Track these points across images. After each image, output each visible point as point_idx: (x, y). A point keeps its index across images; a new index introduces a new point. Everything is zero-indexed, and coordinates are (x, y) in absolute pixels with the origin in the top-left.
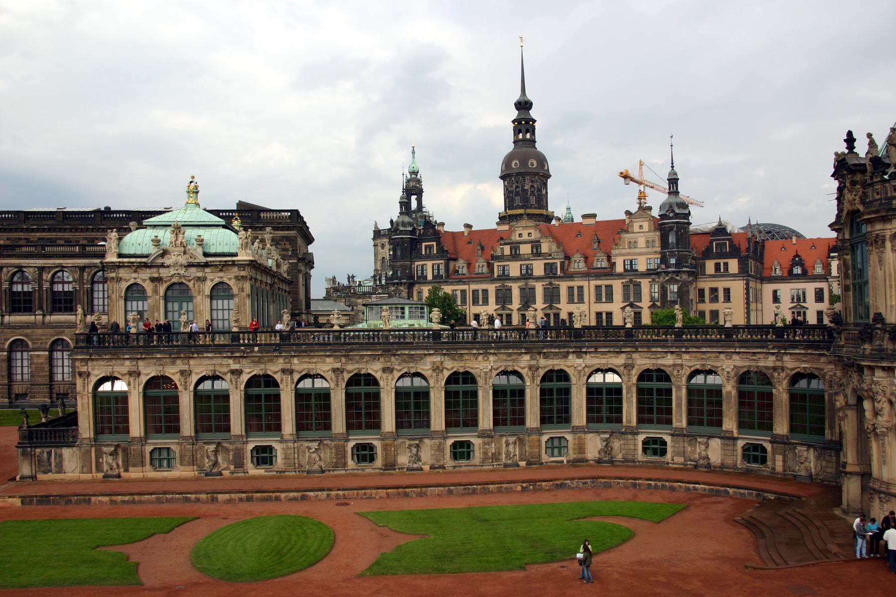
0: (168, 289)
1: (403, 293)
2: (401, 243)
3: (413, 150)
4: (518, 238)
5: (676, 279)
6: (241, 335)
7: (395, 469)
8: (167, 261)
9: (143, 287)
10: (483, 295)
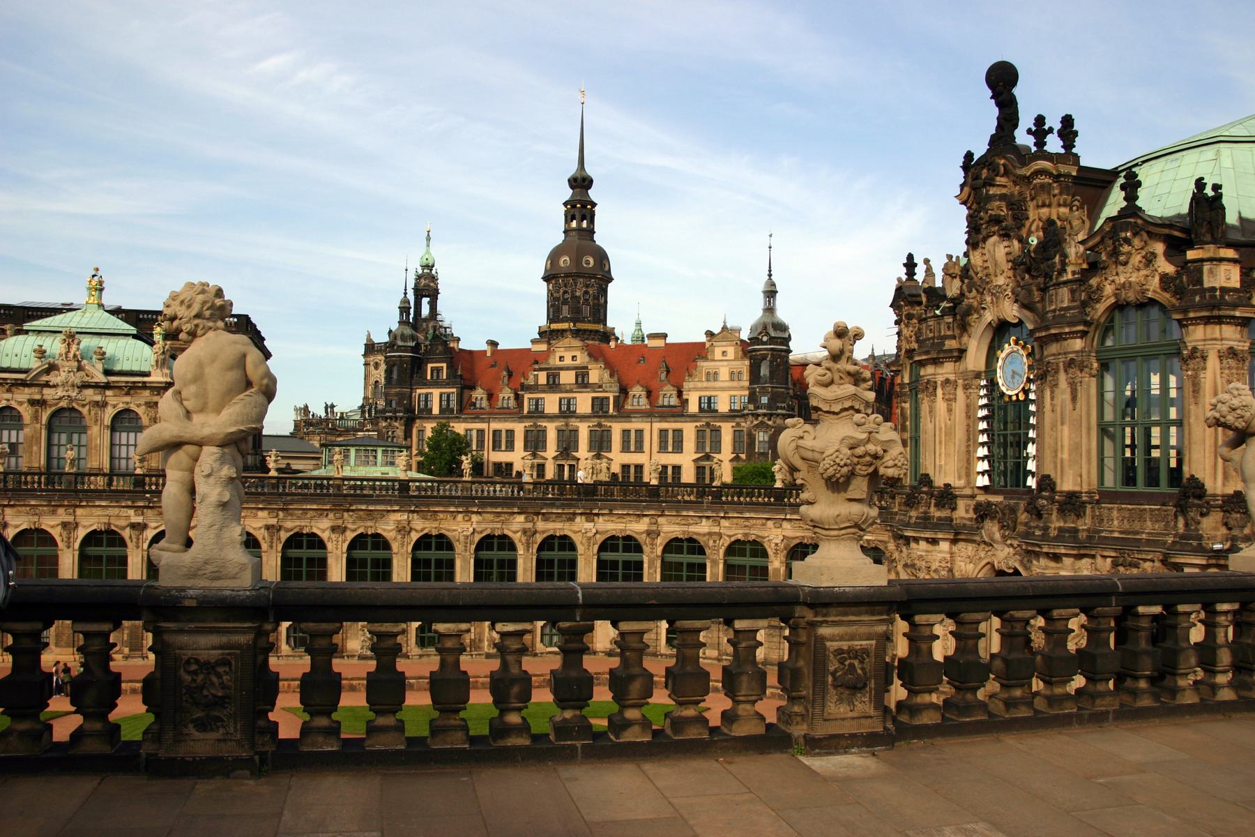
0: (54, 415)
1: (398, 430)
2: (398, 362)
3: (428, 235)
4: (558, 363)
5: (768, 424)
6: (147, 479)
7: (343, 657)
8: (54, 378)
9: (19, 412)
10: (507, 437)
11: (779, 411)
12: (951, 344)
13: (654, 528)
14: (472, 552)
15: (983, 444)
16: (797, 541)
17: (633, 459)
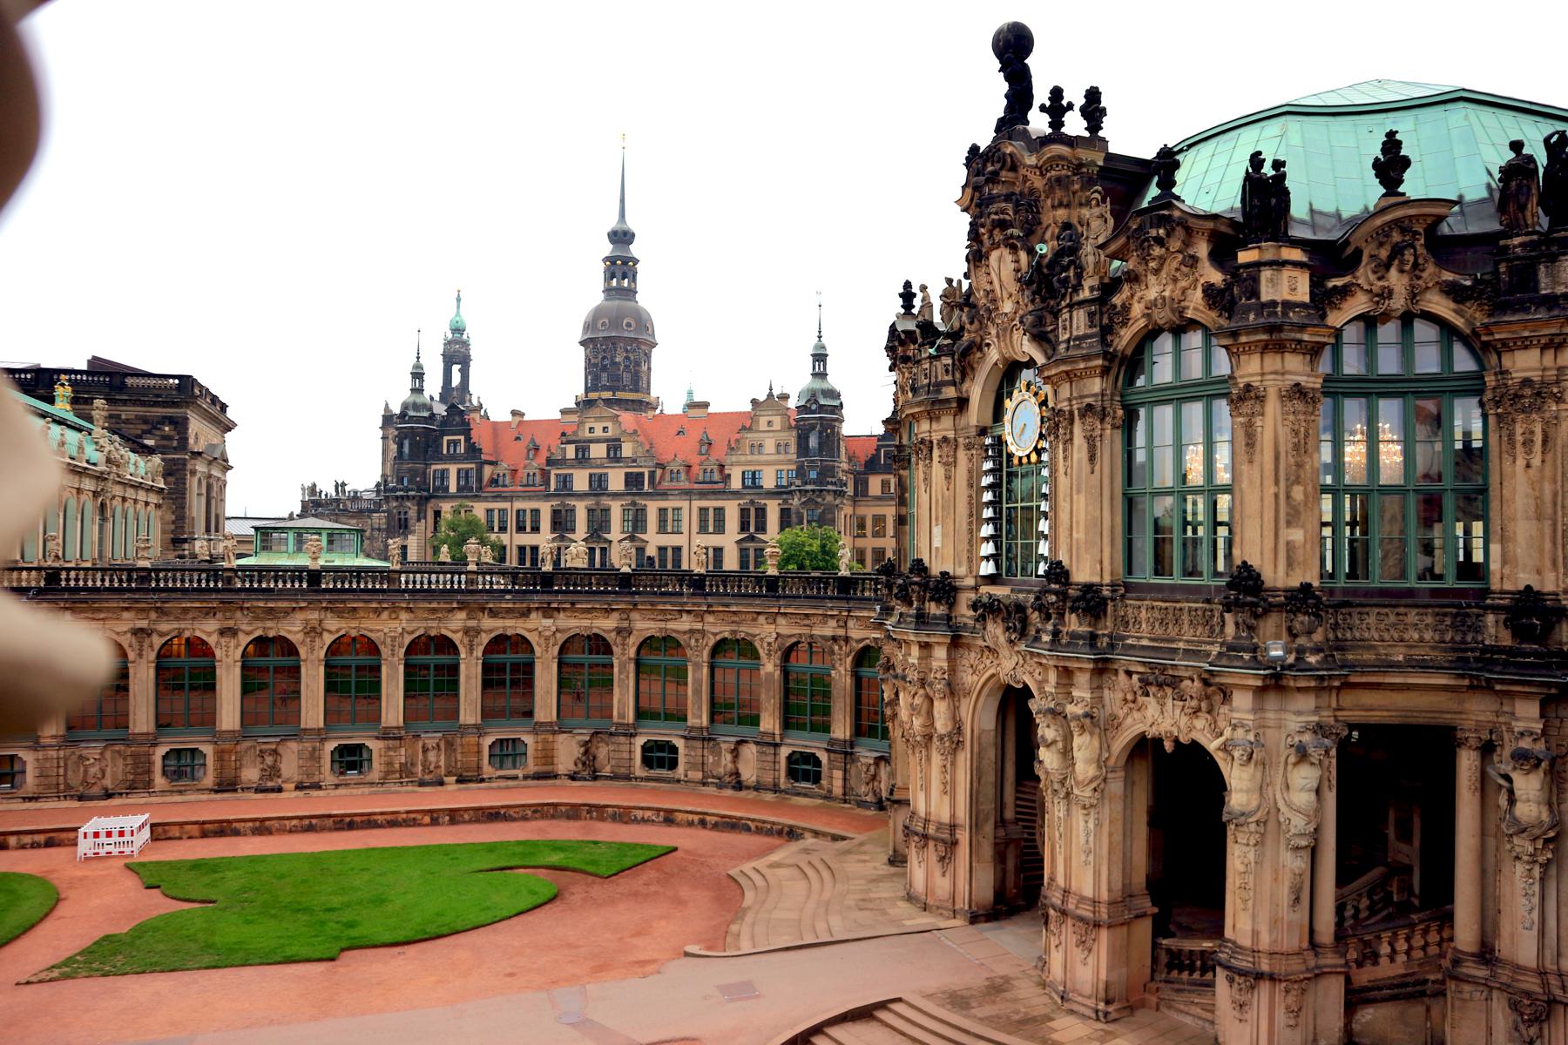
4: (588, 435)
11: (830, 487)
12: (950, 392)
13: (626, 624)
14: (402, 656)
15: (988, 520)
16: (794, 640)
17: (670, 540)
